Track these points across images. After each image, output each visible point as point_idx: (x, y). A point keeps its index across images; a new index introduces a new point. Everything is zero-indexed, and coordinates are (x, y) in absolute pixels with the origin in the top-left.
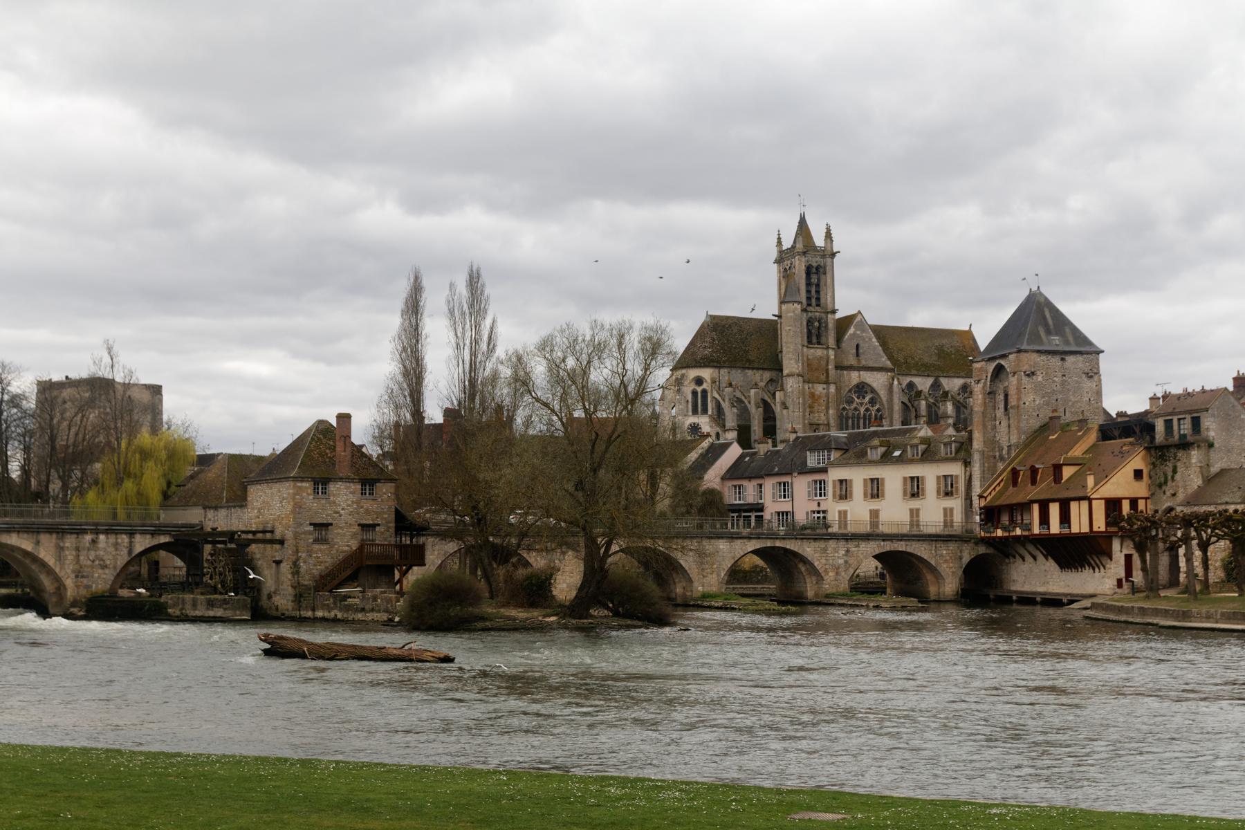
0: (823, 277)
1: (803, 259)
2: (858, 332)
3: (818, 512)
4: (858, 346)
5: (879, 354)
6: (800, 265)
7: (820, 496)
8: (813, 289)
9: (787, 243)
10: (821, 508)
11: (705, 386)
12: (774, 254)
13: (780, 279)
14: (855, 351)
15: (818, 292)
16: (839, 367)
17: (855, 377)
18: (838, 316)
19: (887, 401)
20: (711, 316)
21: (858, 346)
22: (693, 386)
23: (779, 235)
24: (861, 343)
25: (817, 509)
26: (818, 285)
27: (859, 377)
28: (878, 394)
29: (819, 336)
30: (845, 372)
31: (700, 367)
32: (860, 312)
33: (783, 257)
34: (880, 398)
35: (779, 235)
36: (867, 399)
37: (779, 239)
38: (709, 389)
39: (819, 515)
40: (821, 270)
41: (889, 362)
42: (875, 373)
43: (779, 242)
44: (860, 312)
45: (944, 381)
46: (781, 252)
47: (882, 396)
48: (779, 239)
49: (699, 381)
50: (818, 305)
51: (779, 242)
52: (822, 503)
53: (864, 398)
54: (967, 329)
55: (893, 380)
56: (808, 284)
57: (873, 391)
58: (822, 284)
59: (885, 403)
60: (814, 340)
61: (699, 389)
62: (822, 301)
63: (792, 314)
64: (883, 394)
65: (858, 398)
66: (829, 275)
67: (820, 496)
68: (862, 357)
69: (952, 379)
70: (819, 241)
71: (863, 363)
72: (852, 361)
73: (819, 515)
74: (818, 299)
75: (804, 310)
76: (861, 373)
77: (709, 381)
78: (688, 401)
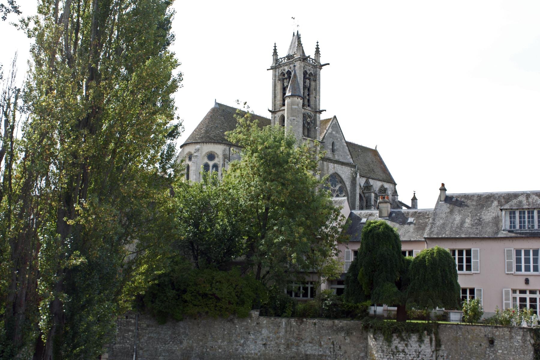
0: (313, 83)
1: (302, 64)
2: (334, 133)
3: (523, 292)
4: (333, 144)
5: (346, 153)
6: (298, 69)
7: (527, 269)
8: (306, 91)
9: (282, 53)
10: (531, 287)
11: (216, 161)
12: (270, 62)
13: (275, 82)
14: (331, 147)
15: (309, 95)
16: (323, 159)
17: (332, 168)
18: (323, 116)
19: (350, 190)
20: (219, 104)
21: (333, 144)
22: (206, 160)
23: (275, 47)
24: (335, 141)
25: (524, 287)
26: (309, 90)
27: (334, 168)
28: (344, 183)
29: (309, 130)
30: (325, 163)
31: (214, 143)
32: (335, 117)
33: (277, 65)
34: (346, 188)
35: (275, 47)
36: (337, 188)
37: (275, 50)
38: (220, 164)
39: (523, 296)
40: (312, 78)
41: (351, 160)
42: (344, 167)
43: (275, 53)
44: (335, 117)
45: (372, 182)
46: (276, 60)
47: (347, 186)
48: (275, 50)
49: (211, 156)
50: (309, 106)
51: (275, 53)
52: (531, 279)
53: (335, 187)
54: (374, 148)
55: (357, 174)
56: (305, 87)
57: (342, 181)
58: (312, 87)
59: (349, 192)
60: (306, 133)
61: (211, 163)
62: (312, 103)
63: (296, 107)
64: (348, 184)
65: (332, 186)
66: (317, 82)
67: (527, 269)
68: (336, 153)
69: (375, 181)
70: (310, 52)
71: (337, 158)
72: (329, 154)
73: (523, 296)
74: (309, 100)
75: (304, 105)
76: (336, 165)
77: (221, 156)
78: (200, 173)
